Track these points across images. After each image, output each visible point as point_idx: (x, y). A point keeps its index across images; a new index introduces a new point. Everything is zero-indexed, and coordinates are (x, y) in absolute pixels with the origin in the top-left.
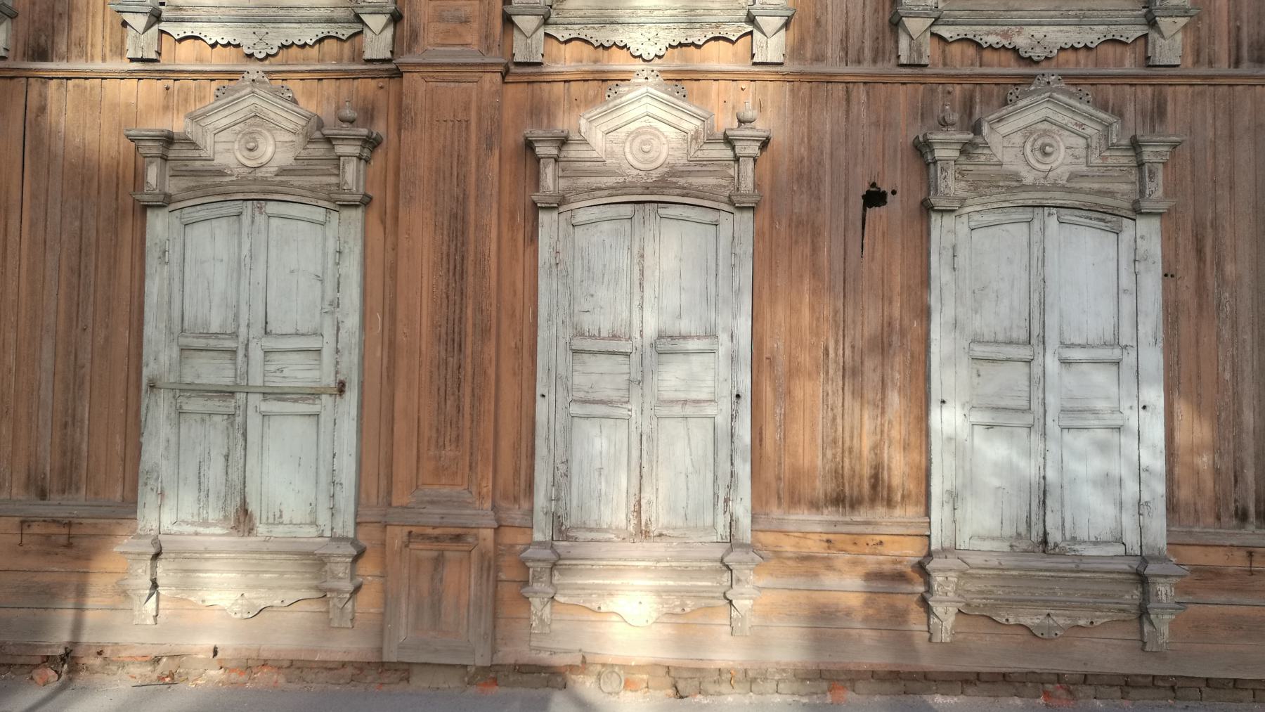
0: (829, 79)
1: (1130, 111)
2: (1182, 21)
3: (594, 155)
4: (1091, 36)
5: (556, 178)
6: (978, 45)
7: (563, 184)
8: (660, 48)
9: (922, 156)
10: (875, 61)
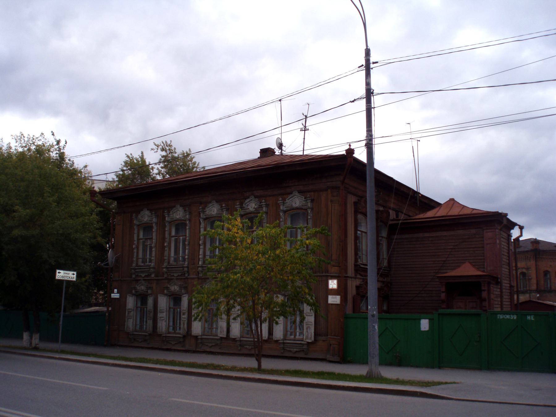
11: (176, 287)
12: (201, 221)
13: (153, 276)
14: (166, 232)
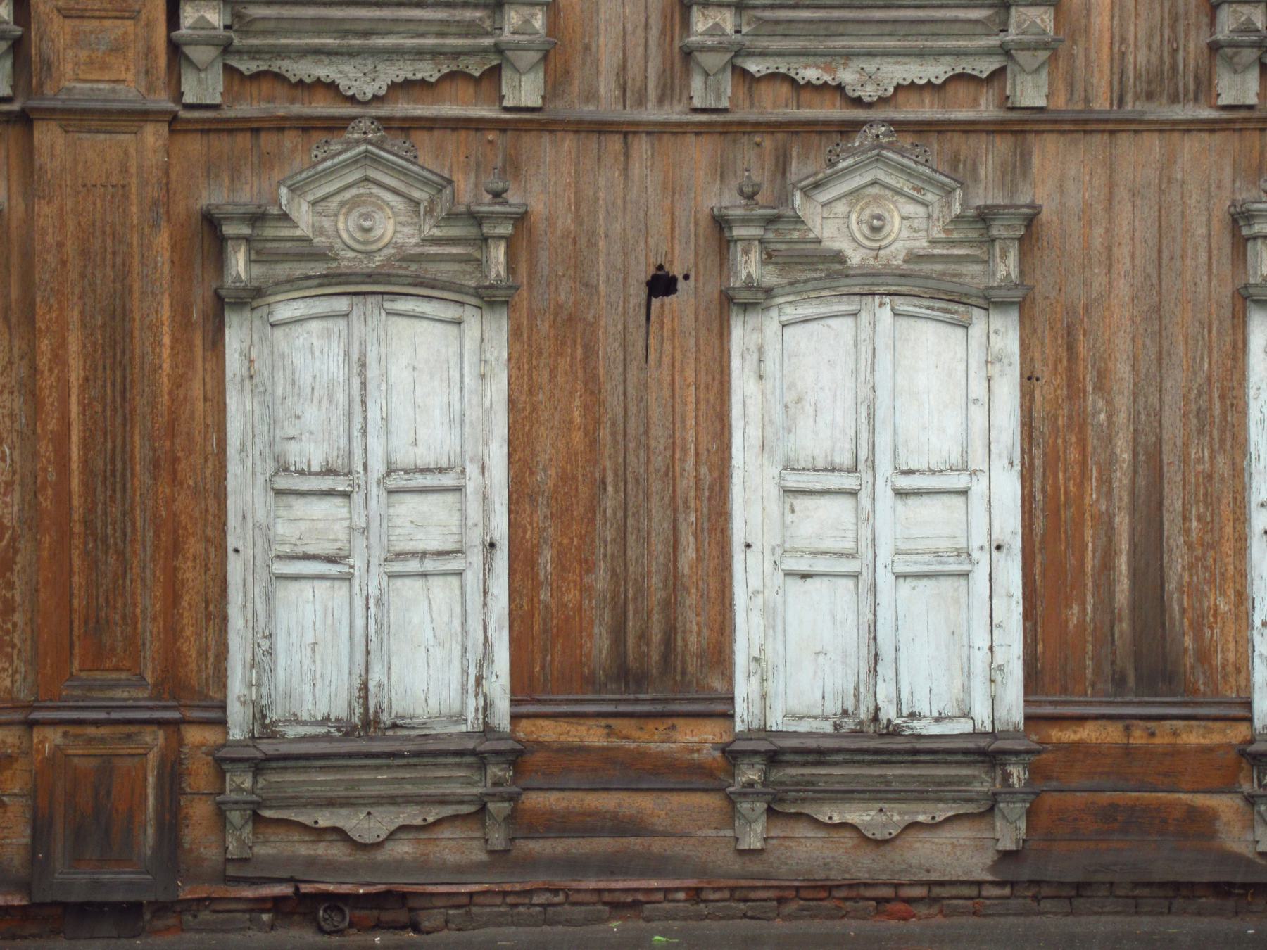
0: (601, 128)
2: (1043, 55)
3: (298, 233)
4: (936, 71)
5: (249, 262)
7: (257, 270)
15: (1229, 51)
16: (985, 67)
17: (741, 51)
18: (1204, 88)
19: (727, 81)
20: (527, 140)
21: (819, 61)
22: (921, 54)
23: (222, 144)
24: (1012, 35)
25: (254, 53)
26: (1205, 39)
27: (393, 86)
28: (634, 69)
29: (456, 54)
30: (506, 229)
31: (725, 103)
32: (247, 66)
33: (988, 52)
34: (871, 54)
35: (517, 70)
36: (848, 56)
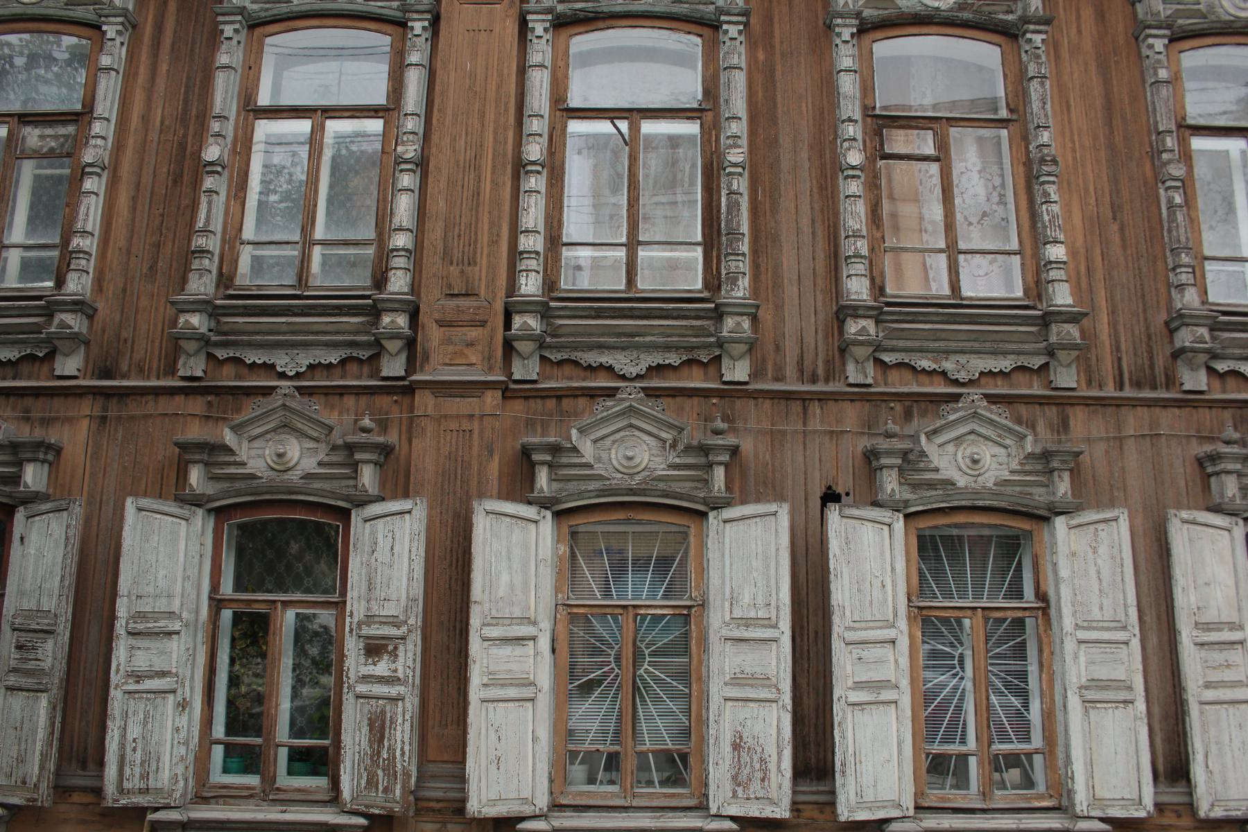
0: (787, 396)
1: (1041, 427)
2: (1075, 353)
3: (584, 460)
4: (1006, 364)
5: (551, 480)
6: (914, 368)
7: (555, 485)
8: (642, 368)
9: (870, 463)
10: (827, 381)
11: (294, 449)
12: (538, 26)
13: (69, 365)
14: (221, 79)
15: (1191, 355)
16: (1036, 362)
17: (879, 348)
18: (1171, 381)
19: (870, 368)
20: (739, 404)
21: (930, 355)
22: (995, 353)
23: (536, 405)
24: (1053, 339)
25: (559, 348)
26: (1168, 351)
27: (650, 368)
28: (809, 357)
29: (692, 348)
30: (725, 458)
31: (869, 381)
32: (555, 356)
33: (1036, 353)
34: (963, 352)
35: (732, 358)
36: (948, 353)
